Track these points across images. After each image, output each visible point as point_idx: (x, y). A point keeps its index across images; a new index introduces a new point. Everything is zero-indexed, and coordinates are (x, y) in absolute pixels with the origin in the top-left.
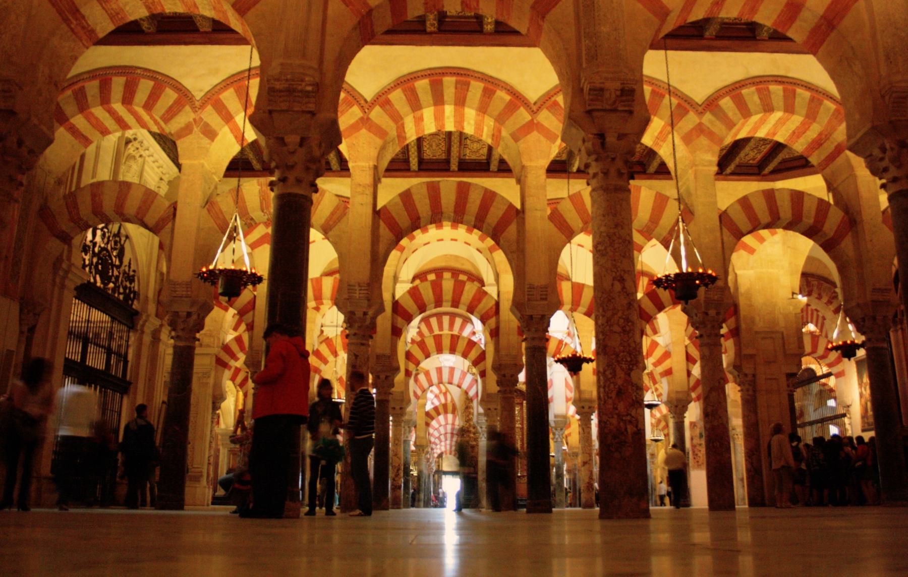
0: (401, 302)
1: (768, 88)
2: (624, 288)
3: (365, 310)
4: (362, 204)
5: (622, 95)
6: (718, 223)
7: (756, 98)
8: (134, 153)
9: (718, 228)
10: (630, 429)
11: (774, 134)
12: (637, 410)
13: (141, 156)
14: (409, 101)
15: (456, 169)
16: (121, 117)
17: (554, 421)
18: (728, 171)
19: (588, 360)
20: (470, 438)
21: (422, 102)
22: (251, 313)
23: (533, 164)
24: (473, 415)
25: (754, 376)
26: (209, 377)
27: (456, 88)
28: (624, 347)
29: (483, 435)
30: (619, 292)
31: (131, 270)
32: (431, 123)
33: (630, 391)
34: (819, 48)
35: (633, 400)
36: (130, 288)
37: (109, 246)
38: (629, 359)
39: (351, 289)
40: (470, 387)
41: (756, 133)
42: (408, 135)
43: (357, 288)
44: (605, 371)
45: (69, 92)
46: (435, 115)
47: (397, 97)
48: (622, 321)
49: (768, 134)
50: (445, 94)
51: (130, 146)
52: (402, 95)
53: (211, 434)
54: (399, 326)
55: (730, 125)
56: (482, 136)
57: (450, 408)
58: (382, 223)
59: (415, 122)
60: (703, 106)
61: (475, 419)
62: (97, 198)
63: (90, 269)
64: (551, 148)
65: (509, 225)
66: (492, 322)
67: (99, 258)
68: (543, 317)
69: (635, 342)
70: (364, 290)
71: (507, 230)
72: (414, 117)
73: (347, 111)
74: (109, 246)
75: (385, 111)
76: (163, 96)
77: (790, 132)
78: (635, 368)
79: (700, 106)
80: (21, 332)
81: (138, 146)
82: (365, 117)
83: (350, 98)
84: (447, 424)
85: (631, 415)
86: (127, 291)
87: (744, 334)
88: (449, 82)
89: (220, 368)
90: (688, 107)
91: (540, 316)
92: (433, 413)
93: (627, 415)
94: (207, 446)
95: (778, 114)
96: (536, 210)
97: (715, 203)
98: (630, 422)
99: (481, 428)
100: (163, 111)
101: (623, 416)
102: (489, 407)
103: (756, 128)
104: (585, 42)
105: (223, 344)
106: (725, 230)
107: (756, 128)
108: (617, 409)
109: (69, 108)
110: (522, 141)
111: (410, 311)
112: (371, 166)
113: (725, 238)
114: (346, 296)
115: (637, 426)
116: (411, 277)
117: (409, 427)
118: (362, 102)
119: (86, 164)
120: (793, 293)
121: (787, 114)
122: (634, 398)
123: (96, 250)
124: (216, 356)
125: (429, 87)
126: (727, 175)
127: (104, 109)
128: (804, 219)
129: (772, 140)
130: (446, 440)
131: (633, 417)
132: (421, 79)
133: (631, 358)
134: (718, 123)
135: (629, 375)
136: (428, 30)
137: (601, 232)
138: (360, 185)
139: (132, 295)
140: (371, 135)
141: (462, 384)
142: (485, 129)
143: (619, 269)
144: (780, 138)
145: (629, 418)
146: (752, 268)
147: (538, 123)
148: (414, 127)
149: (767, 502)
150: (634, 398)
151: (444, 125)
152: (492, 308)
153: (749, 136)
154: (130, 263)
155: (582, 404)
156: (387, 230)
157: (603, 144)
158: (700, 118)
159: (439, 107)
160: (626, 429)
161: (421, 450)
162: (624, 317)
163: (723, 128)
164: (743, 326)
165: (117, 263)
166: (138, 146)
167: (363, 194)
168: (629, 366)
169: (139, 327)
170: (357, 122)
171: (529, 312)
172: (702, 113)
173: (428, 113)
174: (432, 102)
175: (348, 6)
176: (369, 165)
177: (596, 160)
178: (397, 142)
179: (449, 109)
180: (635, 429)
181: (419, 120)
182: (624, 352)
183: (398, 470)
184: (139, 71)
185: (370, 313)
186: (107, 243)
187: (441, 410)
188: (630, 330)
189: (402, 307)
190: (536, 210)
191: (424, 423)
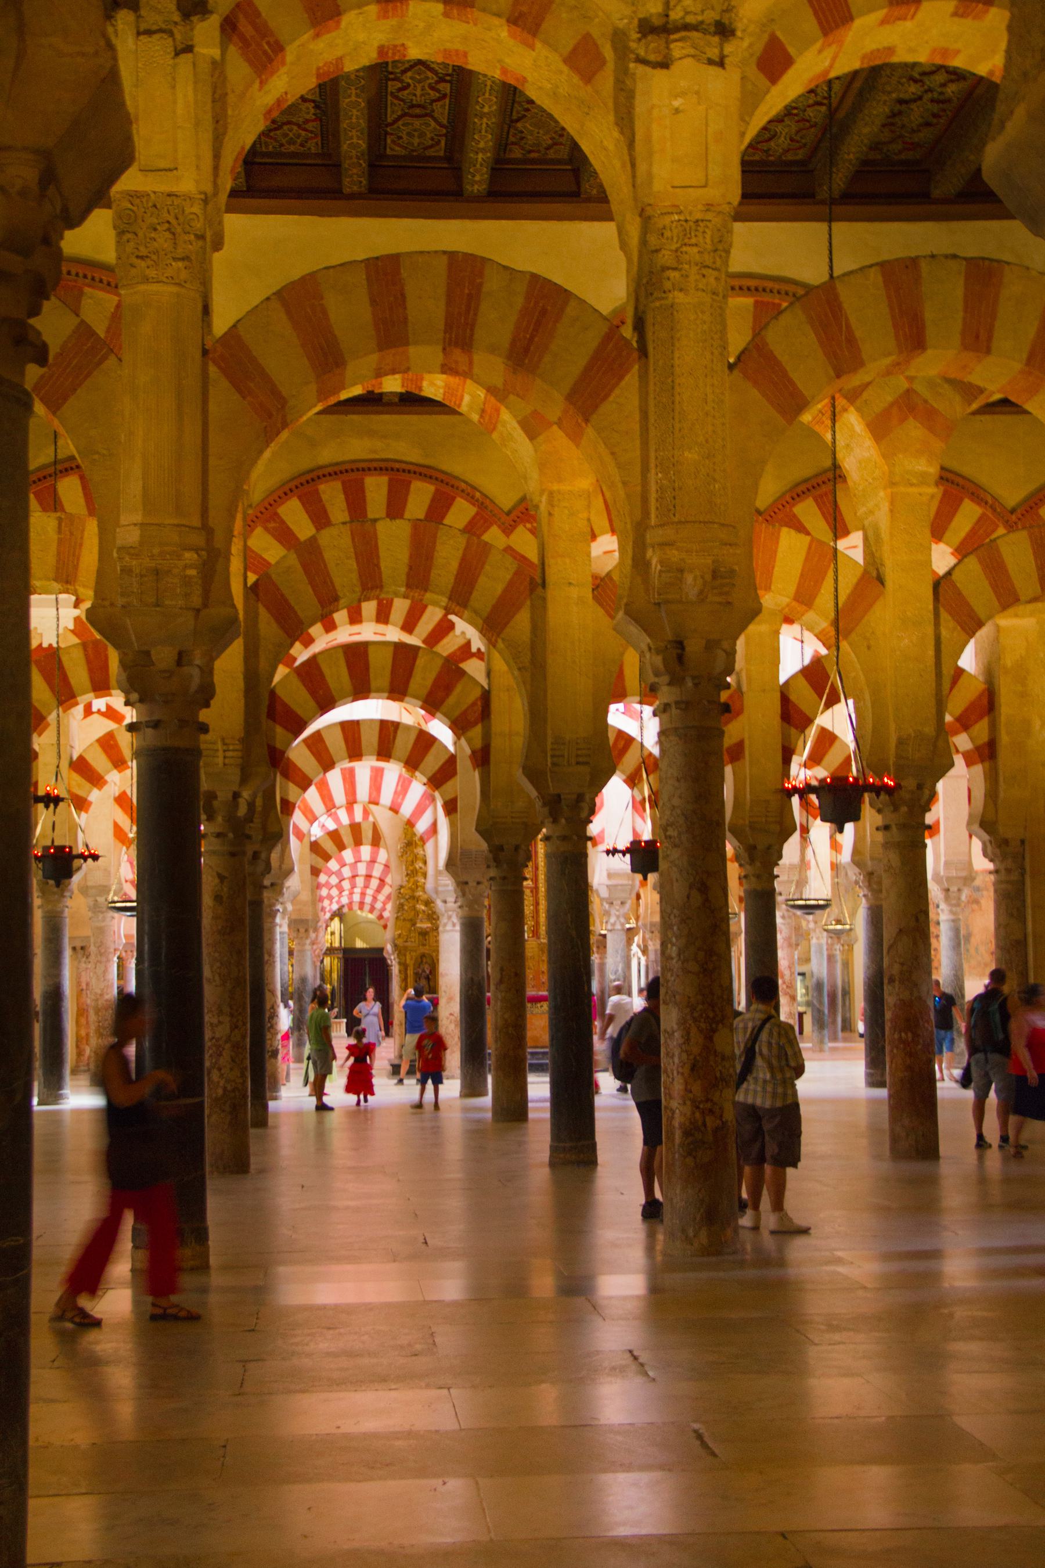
0: (279, 692)
2: (707, 900)
3: (235, 788)
20: (417, 913)
23: (565, 487)
24: (425, 875)
29: (449, 917)
33: (712, 1063)
38: (711, 1015)
40: (419, 811)
43: (220, 746)
54: (279, 745)
56: (459, 406)
57: (367, 834)
58: (263, 612)
61: (430, 884)
65: (519, 609)
66: (477, 731)
68: (580, 798)
69: (721, 986)
70: (233, 750)
71: (512, 624)
84: (358, 860)
85: (712, 1101)
91: (574, 797)
92: (329, 846)
93: (707, 1100)
97: (929, 562)
98: (711, 1111)
99: (445, 902)
101: (700, 1102)
102: (465, 878)
106: (944, 615)
111: (299, 712)
113: (944, 633)
122: (718, 1075)
131: (715, 1104)
136: (347, 190)
137: (674, 807)
141: (400, 805)
145: (709, 1105)
150: (718, 1075)
152: (474, 704)
156: (274, 625)
157: (680, 658)
160: (705, 1125)
161: (302, 930)
171: (552, 790)
175: (244, 398)
180: (718, 1122)
185: (246, 794)
187: (347, 838)
189: (285, 705)
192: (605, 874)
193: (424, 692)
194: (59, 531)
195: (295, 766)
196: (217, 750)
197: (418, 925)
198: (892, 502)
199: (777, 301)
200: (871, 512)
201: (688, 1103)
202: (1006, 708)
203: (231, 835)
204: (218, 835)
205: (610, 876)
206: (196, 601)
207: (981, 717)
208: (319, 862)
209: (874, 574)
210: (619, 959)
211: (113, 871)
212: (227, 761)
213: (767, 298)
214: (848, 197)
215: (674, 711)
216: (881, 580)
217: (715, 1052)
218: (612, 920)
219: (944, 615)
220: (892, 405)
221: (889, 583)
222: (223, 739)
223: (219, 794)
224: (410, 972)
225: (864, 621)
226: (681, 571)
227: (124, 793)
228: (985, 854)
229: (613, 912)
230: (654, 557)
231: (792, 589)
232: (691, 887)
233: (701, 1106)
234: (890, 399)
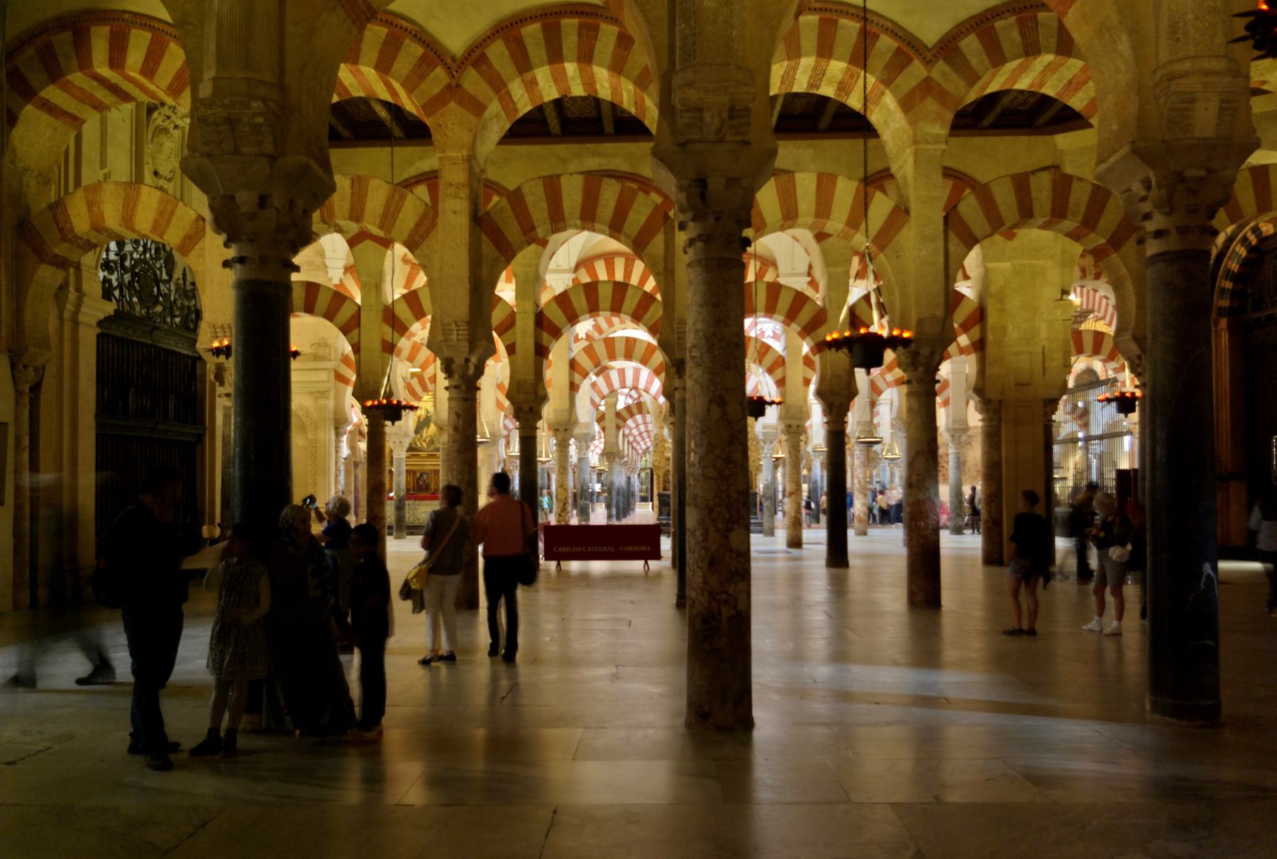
0: (546, 312)
1: (1035, 17)
2: (725, 413)
4: (455, 212)
5: (731, 117)
6: (942, 228)
7: (1016, 35)
8: (165, 124)
9: (942, 235)
10: (726, 612)
11: (1042, 85)
13: (176, 127)
14: (513, 55)
15: (612, 132)
16: (116, 84)
17: (763, 433)
18: (986, 122)
19: (772, 403)
21: (532, 59)
22: (356, 332)
26: (327, 398)
27: (580, 35)
31: (188, 283)
32: (550, 87)
34: (1070, 7)
36: (189, 307)
37: (148, 255)
38: (727, 516)
39: (446, 332)
41: (1015, 82)
42: (520, 106)
43: (454, 326)
44: (695, 531)
45: (30, 51)
46: (553, 76)
47: (498, 52)
49: (1032, 85)
50: (564, 46)
51: (155, 115)
52: (504, 50)
53: (336, 465)
54: (545, 343)
55: (972, 78)
58: (484, 237)
59: (527, 88)
60: (934, 51)
62: (95, 209)
63: (121, 292)
67: (134, 275)
70: (463, 330)
72: (523, 81)
73: (428, 75)
74: (148, 255)
75: (481, 73)
76: (166, 57)
78: (736, 527)
79: (930, 50)
80: (19, 393)
81: (170, 113)
82: (454, 85)
83: (431, 55)
85: (727, 592)
86: (186, 311)
87: (991, 350)
88: (570, 25)
89: (341, 385)
90: (911, 53)
92: (625, 414)
94: (333, 479)
95: (1048, 58)
98: (726, 602)
100: (169, 79)
103: (1015, 76)
104: (680, 27)
105: (343, 355)
106: (952, 236)
109: (34, 78)
111: (557, 323)
112: (465, 158)
113: (952, 248)
114: (441, 338)
115: (735, 607)
116: (573, 264)
117: (586, 442)
118: (449, 61)
119: (85, 150)
121: (1059, 57)
122: (733, 569)
123: (127, 263)
124: (335, 371)
125: (541, 35)
127: (86, 74)
129: (1037, 93)
130: (643, 439)
131: (730, 595)
132: (531, 23)
134: (954, 77)
135: (727, 538)
138: (451, 184)
139: (193, 316)
140: (464, 111)
142: (625, 94)
144: (1049, 91)
145: (724, 596)
146: (1008, 260)
148: (526, 95)
150: (733, 569)
151: (569, 88)
153: (1005, 88)
154: (184, 275)
155: (789, 422)
156: (492, 247)
157: (703, 196)
158: (929, 71)
159: (557, 66)
160: (720, 612)
163: (961, 83)
164: (990, 337)
165: (165, 277)
166: (170, 113)
167: (455, 197)
170: (442, 91)
171: (678, 356)
172: (931, 61)
173: (542, 74)
174: (545, 58)
176: (462, 156)
177: (694, 219)
178: (504, 116)
179: (571, 68)
181: (531, 85)
183: (565, 504)
184: (126, 16)
185: (474, 359)
186: (144, 252)
191: (614, 425)
192: (761, 427)
193: (631, 311)
194: (352, 187)
195: (578, 363)
196: (452, 330)
197: (666, 455)
198: (916, 156)
199: (835, 17)
200: (901, 167)
201: (706, 594)
202: (992, 319)
203: (464, 387)
204: (456, 387)
205: (764, 427)
206: (268, 148)
207: (975, 324)
208: (621, 423)
209: (903, 208)
210: (769, 472)
211: (496, 424)
212: (460, 337)
213: (827, 15)
215: (699, 244)
216: (907, 212)
218: (766, 451)
219: (952, 236)
220: (916, 88)
221: (913, 214)
222: (456, 322)
223: (455, 359)
224: (661, 479)
225: (896, 239)
226: (700, 110)
227: (502, 383)
228: (976, 410)
229: (766, 447)
230: (676, 100)
231: (845, 217)
232: (711, 401)
233: (717, 597)
234: (914, 84)
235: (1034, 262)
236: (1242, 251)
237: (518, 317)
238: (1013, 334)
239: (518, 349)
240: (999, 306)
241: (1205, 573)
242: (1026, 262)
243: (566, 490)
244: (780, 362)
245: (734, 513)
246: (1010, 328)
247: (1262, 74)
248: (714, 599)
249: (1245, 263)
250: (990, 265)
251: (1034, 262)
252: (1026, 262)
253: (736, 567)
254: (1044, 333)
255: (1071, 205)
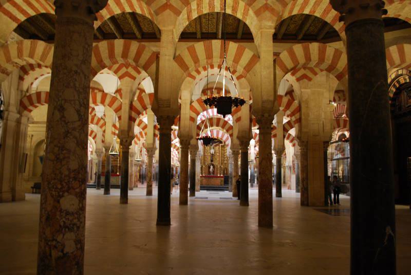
6: (272, 63)
10: (55, 254)
11: (314, 12)
12: (64, 235)
23: (165, 29)
25: (307, 142)
28: (55, 174)
30: (58, 121)
33: (58, 217)
35: (60, 226)
38: (59, 187)
48: (57, 149)
64: (176, 19)
77: (323, 10)
85: (56, 240)
87: (303, 122)
93: (53, 240)
96: (166, 55)
98: (55, 247)
103: (303, 8)
107: (303, 8)
108: (45, 234)
110: (160, 15)
113: (277, 72)
115: (62, 251)
120: (330, 101)
122: (62, 224)
126: (299, 40)
128: (326, 61)
131: (58, 242)
133: (62, 185)
135: (58, 202)
143: (60, 99)
145: (54, 243)
146: (310, 88)
147: (170, 4)
149: (310, 204)
150: (62, 224)
160: (50, 255)
162: (59, 145)
164: (303, 117)
168: (59, 193)
169: (5, 118)
180: (60, 254)
182: (55, 179)
188: (64, 158)
190: (166, 55)
194: (31, 44)
201: (43, 240)
202: (303, 110)
207: (297, 112)
214: (282, 39)
217: (61, 209)
219: (277, 67)
221: (261, 57)
228: (299, 145)
232: (55, 108)
233: (49, 243)
234: (261, 5)
235: (319, 90)
236: (394, 90)
237: (123, 105)
238: (312, 116)
239: (122, 118)
240: (306, 106)
241: (388, 233)
242: (316, 89)
243: (151, 173)
244: (231, 128)
245: (65, 184)
246: (310, 114)
247: (398, 12)
248: (47, 244)
249: (395, 94)
250: (302, 90)
251: (319, 90)
252: (316, 89)
253: (64, 222)
254: (323, 116)
255: (326, 57)
